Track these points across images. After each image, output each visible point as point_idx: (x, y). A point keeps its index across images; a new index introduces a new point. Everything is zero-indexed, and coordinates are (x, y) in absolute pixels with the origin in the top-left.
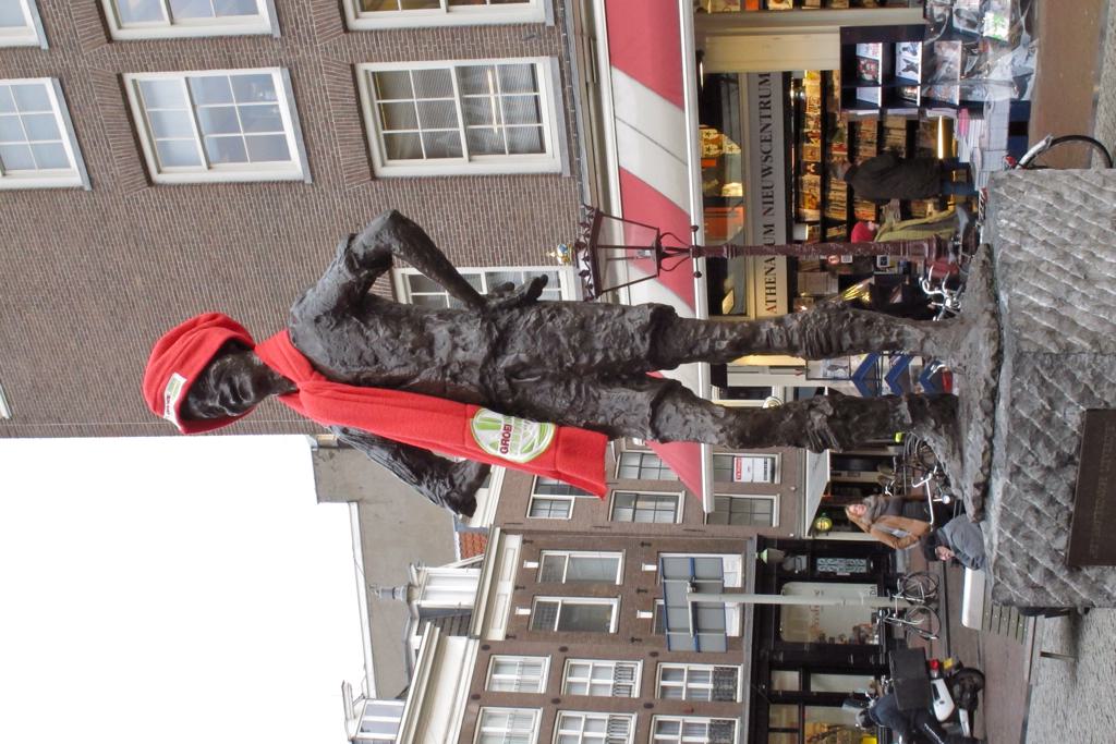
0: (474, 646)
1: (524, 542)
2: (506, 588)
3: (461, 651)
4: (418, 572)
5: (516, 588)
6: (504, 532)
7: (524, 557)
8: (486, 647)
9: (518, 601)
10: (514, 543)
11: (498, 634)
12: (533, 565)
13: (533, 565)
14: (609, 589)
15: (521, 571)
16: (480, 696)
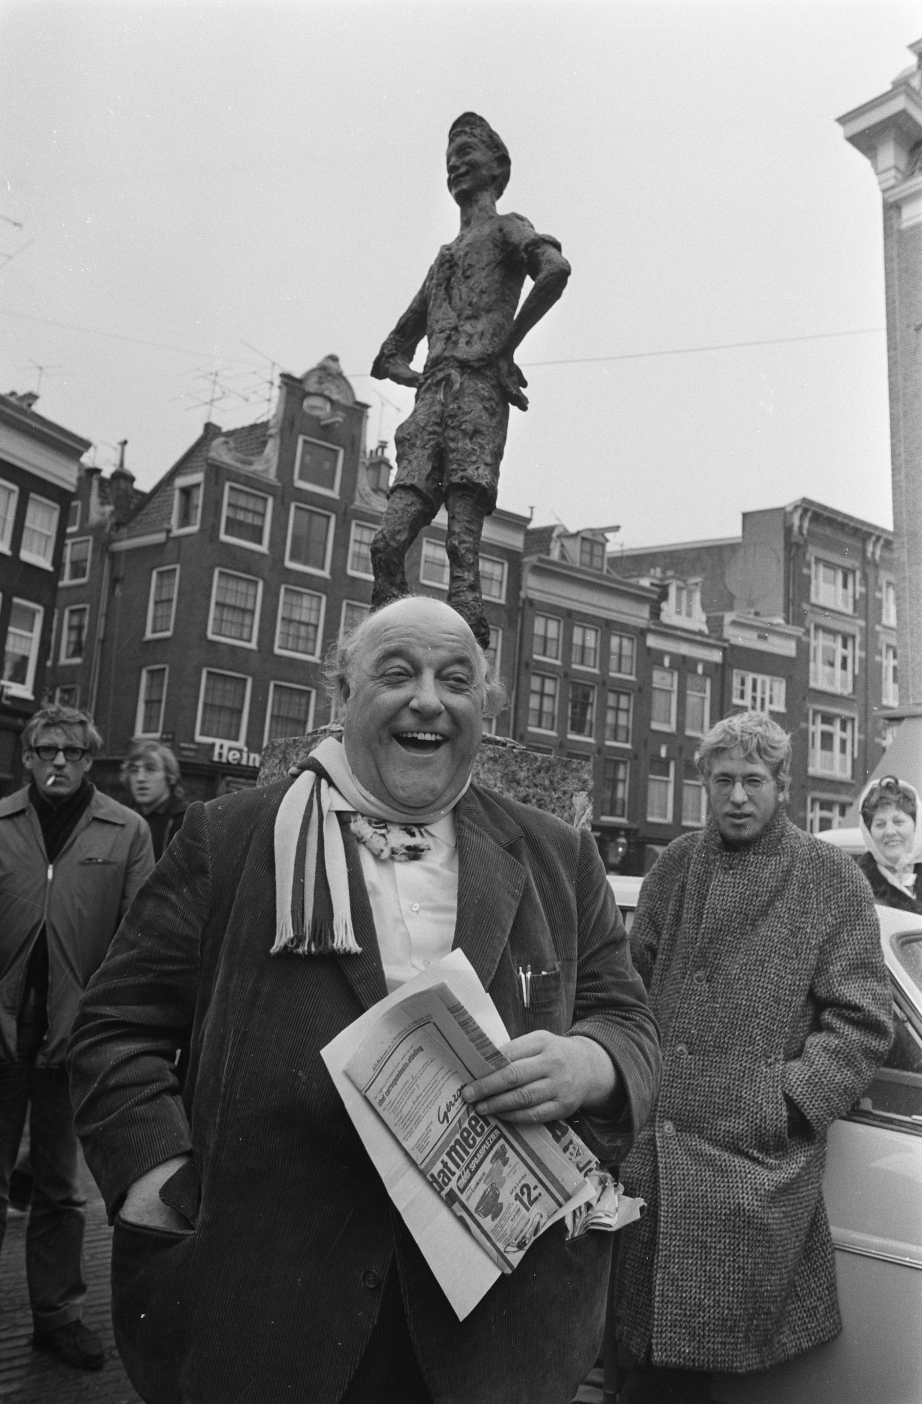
0: (642, 623)
1: (716, 664)
2: (685, 649)
3: (639, 615)
4: (696, 584)
5: (684, 657)
6: (724, 650)
7: (707, 664)
8: (643, 633)
9: (675, 657)
10: (716, 656)
11: (652, 641)
12: (700, 669)
13: (700, 669)
14: (681, 725)
15: (695, 661)
16: (607, 627)
